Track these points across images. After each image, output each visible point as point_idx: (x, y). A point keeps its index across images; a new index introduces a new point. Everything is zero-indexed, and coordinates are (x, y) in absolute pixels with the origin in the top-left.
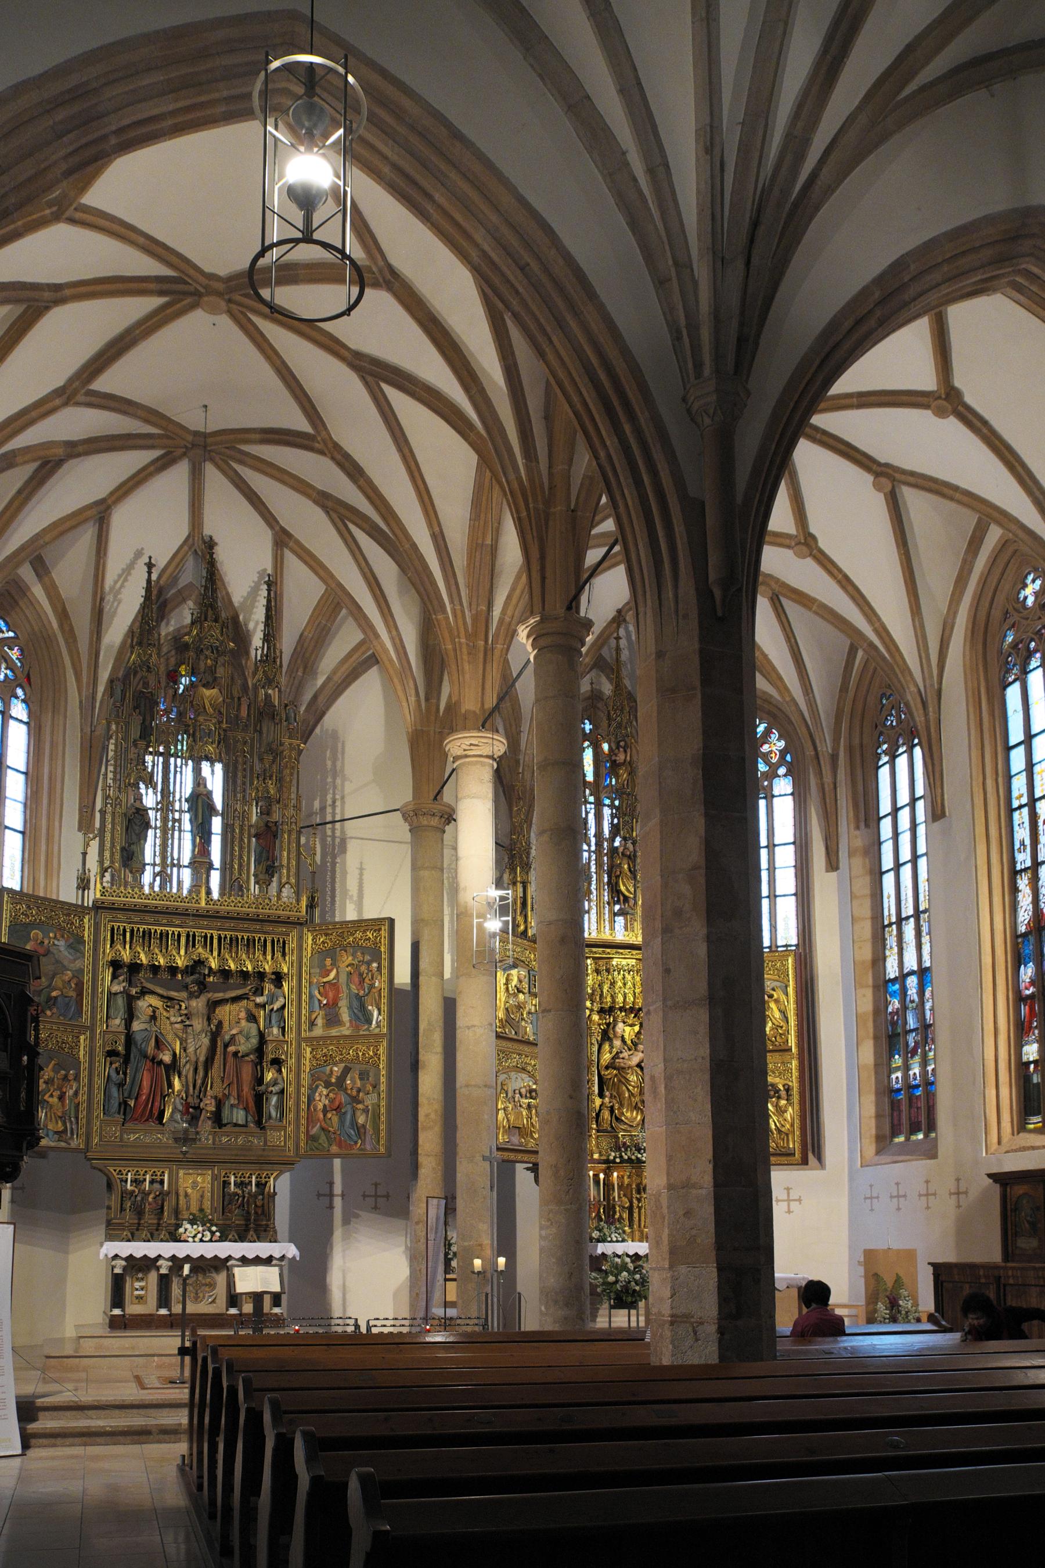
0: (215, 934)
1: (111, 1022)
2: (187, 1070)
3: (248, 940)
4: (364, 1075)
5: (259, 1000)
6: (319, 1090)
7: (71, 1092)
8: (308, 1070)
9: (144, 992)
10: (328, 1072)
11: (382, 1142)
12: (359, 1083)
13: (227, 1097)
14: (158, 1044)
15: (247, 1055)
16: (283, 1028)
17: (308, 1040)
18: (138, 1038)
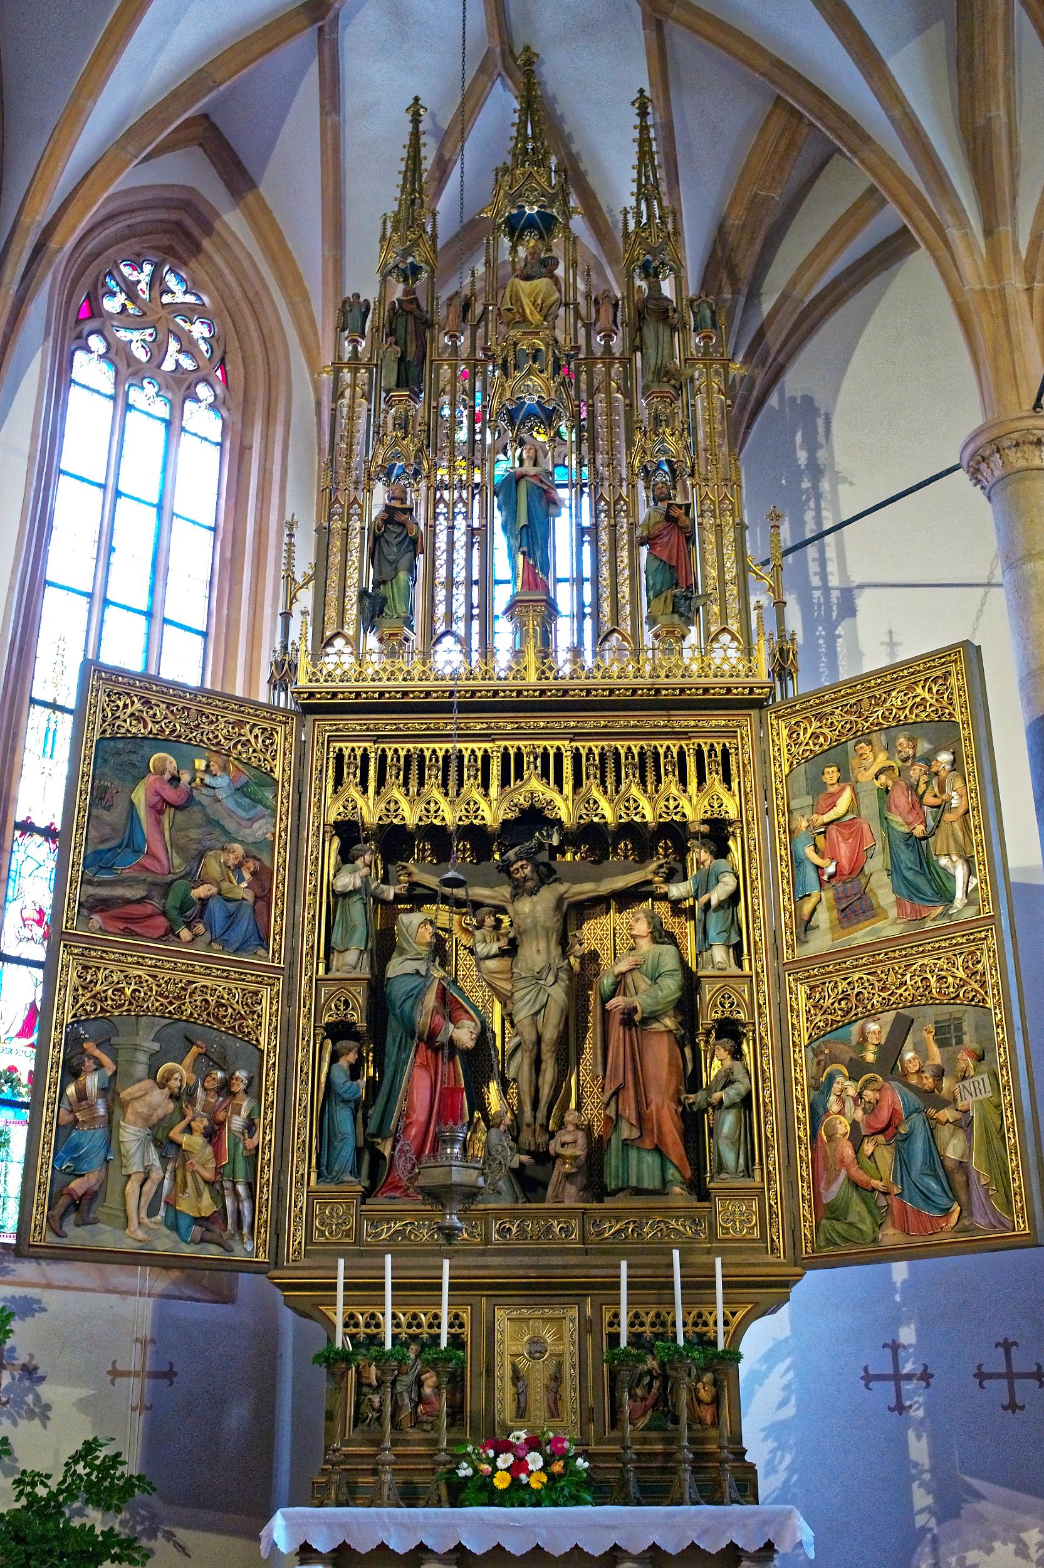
0: (564, 745)
3: (642, 755)
4: (947, 1034)
5: (676, 890)
6: (836, 1087)
7: (237, 1123)
8: (805, 1040)
9: (417, 897)
10: (855, 1039)
11: (1018, 1204)
12: (936, 1056)
13: (612, 1123)
15: (654, 1017)
16: (738, 948)
17: (799, 967)
18: (397, 991)
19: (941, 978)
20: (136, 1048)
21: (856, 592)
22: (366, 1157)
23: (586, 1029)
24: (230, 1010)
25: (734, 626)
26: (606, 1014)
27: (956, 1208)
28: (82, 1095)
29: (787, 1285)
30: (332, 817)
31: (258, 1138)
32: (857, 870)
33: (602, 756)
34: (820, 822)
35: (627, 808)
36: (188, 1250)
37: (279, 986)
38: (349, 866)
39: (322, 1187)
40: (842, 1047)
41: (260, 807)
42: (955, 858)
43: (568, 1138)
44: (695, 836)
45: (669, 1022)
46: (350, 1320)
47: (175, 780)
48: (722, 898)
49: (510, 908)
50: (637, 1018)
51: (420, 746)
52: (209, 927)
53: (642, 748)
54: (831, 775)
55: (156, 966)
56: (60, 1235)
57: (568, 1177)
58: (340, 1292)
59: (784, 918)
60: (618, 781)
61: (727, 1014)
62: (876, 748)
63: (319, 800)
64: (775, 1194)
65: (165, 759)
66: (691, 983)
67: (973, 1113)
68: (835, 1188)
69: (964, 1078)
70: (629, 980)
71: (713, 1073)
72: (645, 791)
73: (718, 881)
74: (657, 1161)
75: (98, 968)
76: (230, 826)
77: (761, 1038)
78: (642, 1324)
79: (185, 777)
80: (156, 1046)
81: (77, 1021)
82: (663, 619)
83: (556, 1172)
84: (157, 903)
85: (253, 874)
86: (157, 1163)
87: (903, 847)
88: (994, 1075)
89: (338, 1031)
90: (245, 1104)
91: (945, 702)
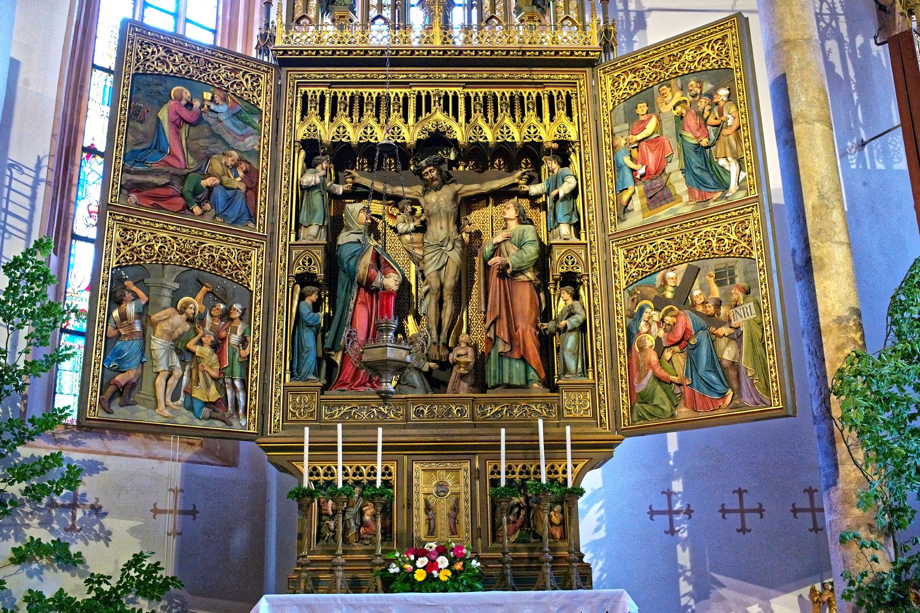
0: (459, 90)
1: (302, 232)
2: (428, 306)
5: (534, 189)
6: (645, 316)
7: (235, 339)
9: (358, 194)
11: (774, 388)
12: (716, 292)
13: (492, 342)
14: (379, 262)
15: (520, 271)
16: (577, 226)
17: (621, 237)
18: (345, 253)
19: (719, 240)
20: (162, 286)
21: (646, 14)
22: (324, 365)
23: (473, 282)
24: (229, 263)
25: (574, 15)
26: (487, 268)
27: (730, 393)
28: (123, 316)
29: (612, 446)
30: (300, 136)
31: (248, 350)
32: (660, 171)
33: (485, 98)
34: (634, 140)
35: (502, 133)
36: (200, 424)
37: (263, 248)
38: (311, 170)
39: (295, 383)
40: (649, 289)
41: (250, 128)
42: (730, 159)
43: (462, 352)
44: (548, 152)
45: (530, 275)
46: (314, 472)
47: (189, 105)
48: (567, 192)
49: (422, 201)
50: (509, 271)
51: (360, 90)
52: (214, 206)
53: (512, 93)
54: (642, 108)
55: (176, 231)
56: (110, 412)
57: (462, 377)
58: (306, 452)
59: (609, 205)
60: (496, 115)
61: (570, 270)
62: (674, 90)
63: (291, 125)
64: (603, 386)
65: (182, 91)
66: (545, 251)
67: (743, 329)
68: (645, 382)
69: (736, 306)
70: (503, 247)
71: (560, 310)
72: (514, 121)
73: (563, 181)
74: (523, 366)
75: (135, 231)
76: (229, 139)
77: (593, 285)
78: (513, 473)
79: (197, 104)
80: (177, 286)
81: (120, 266)
82: (526, 9)
83: (454, 374)
84: (177, 188)
85: (245, 172)
86: (178, 365)
87: (693, 154)
88: (757, 304)
89: (305, 280)
90: (240, 326)
91: (723, 56)
